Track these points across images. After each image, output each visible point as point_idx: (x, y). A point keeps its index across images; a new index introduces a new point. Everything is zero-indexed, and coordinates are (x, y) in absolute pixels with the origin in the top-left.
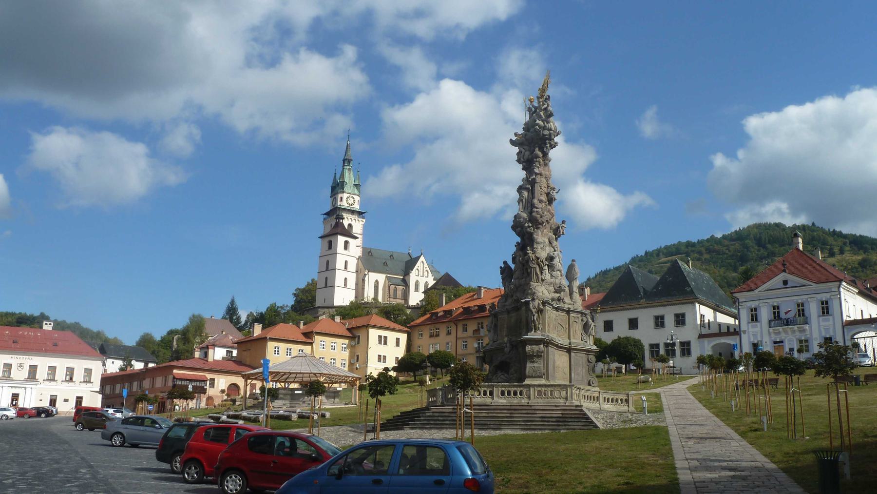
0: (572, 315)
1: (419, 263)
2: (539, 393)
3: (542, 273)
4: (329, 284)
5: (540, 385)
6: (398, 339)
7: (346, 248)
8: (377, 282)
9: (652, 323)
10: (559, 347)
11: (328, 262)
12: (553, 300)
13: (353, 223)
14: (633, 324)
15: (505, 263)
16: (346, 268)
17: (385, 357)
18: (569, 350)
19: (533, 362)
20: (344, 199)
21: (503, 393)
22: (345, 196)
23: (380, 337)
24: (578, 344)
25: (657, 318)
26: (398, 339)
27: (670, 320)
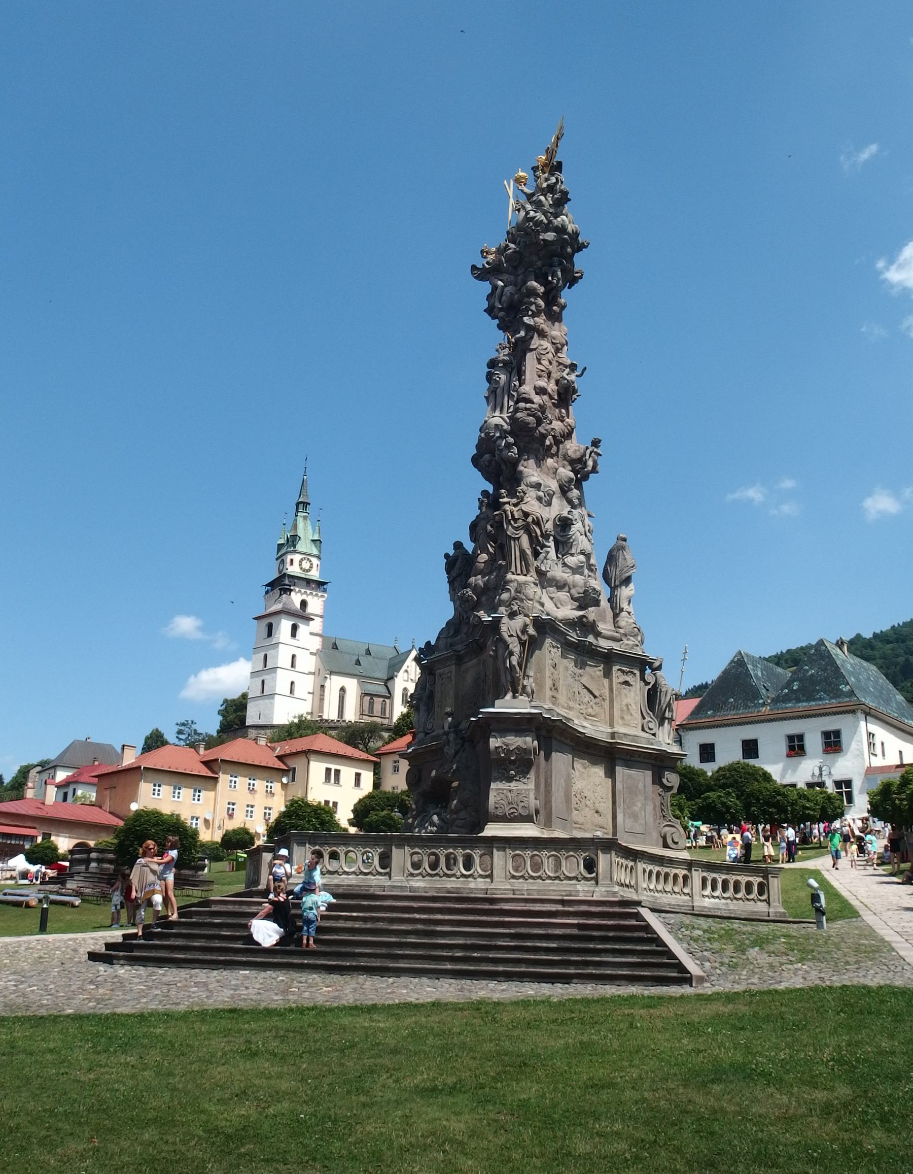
3: (536, 554)
4: (266, 694)
6: (358, 775)
7: (294, 634)
8: (343, 690)
9: (783, 747)
13: (309, 599)
14: (750, 748)
15: (458, 545)
16: (293, 665)
19: (510, 779)
20: (296, 563)
22: (297, 558)
23: (328, 770)
25: (791, 738)
26: (358, 775)
27: (813, 742)
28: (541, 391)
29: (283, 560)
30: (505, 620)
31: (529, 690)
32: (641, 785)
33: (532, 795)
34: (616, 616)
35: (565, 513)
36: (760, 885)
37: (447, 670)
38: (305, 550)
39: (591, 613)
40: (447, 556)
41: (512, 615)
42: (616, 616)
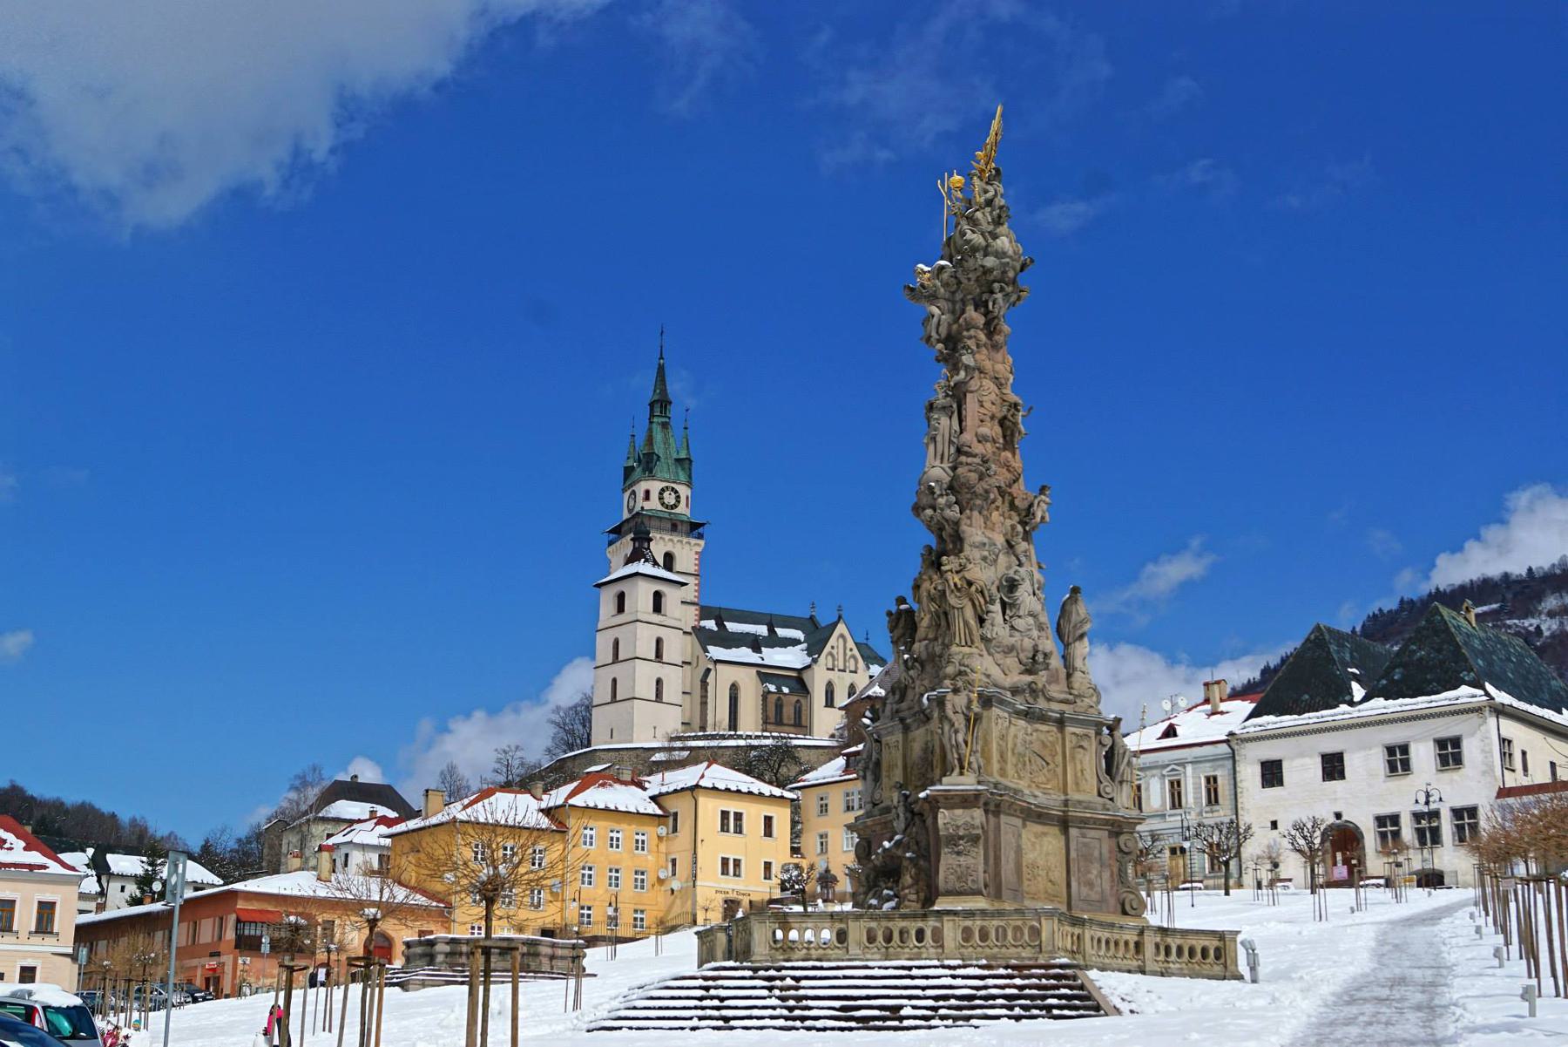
0: (1069, 729)
2: (967, 934)
3: (981, 621)
5: (970, 914)
6: (768, 820)
7: (657, 608)
8: (734, 688)
9: (1379, 760)
10: (1037, 815)
11: (616, 643)
12: (1015, 691)
14: (1333, 767)
16: (659, 655)
17: (737, 863)
18: (1064, 824)
19: (959, 853)
20: (654, 496)
21: (871, 939)
22: (655, 486)
23: (725, 814)
24: (1087, 806)
25: (1391, 750)
26: (768, 820)
27: (1423, 755)
28: (982, 439)
29: (634, 493)
30: (950, 696)
31: (975, 766)
32: (1096, 853)
33: (981, 868)
34: (1069, 676)
35: (1011, 573)
36: (1217, 950)
39: (1041, 678)
40: (889, 614)
41: (956, 691)
42: (1069, 676)
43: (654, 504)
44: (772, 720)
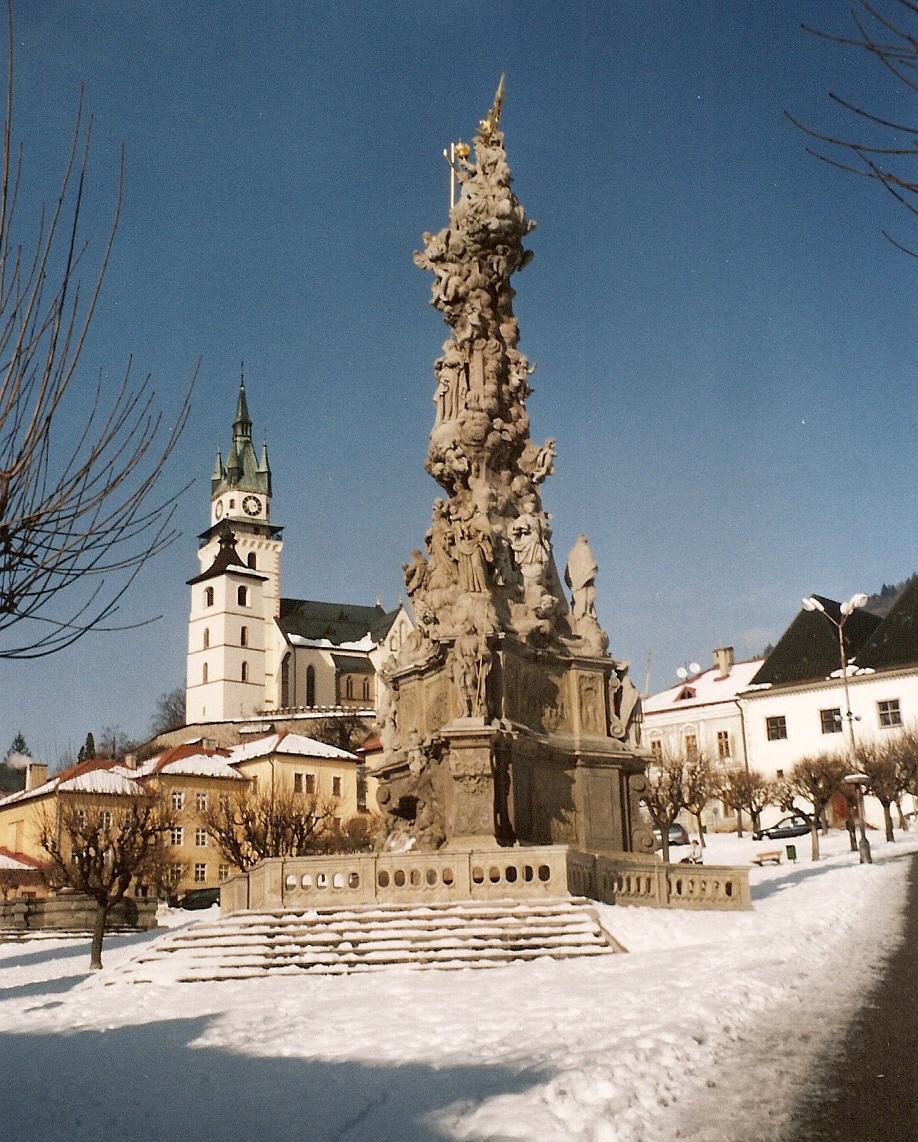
1: (396, 626)
7: (242, 601)
16: (243, 642)
22: (238, 496)
23: (298, 777)
25: (883, 705)
37: (410, 685)
38: (249, 487)
43: (237, 513)
44: (344, 695)
